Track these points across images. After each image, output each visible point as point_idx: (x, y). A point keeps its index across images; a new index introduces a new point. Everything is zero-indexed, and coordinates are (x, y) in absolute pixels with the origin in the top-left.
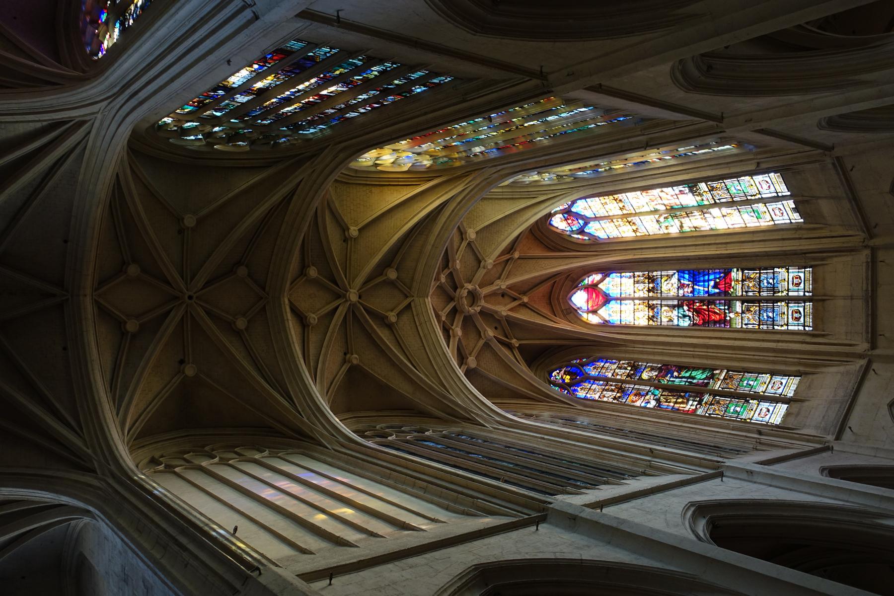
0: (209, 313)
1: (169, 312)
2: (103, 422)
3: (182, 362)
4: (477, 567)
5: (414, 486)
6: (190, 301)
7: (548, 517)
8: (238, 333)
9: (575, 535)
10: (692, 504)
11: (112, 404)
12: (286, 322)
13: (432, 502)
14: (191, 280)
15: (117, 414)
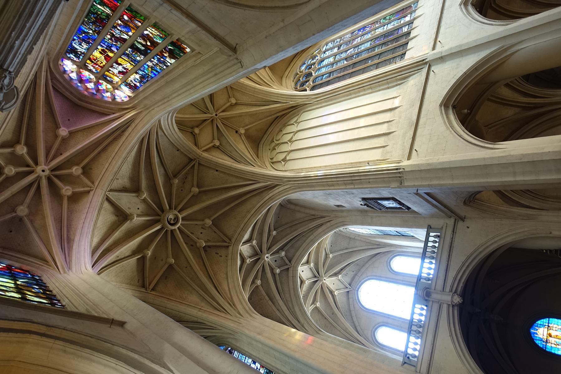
0: (223, 111)
1: (217, 125)
2: (247, 170)
3: (237, 132)
4: (441, 106)
5: (365, 90)
6: (218, 116)
7: (431, 64)
8: (236, 104)
9: (447, 63)
10: (460, 5)
11: (247, 166)
12: (244, 83)
13: (379, 90)
14: (208, 110)
15: (254, 166)
